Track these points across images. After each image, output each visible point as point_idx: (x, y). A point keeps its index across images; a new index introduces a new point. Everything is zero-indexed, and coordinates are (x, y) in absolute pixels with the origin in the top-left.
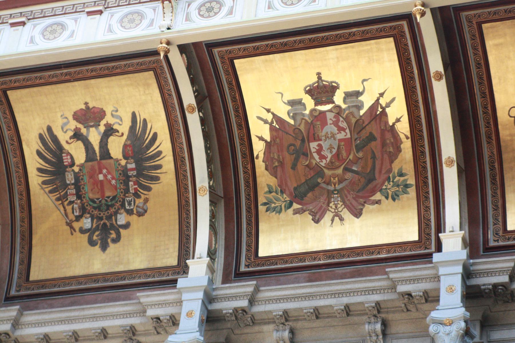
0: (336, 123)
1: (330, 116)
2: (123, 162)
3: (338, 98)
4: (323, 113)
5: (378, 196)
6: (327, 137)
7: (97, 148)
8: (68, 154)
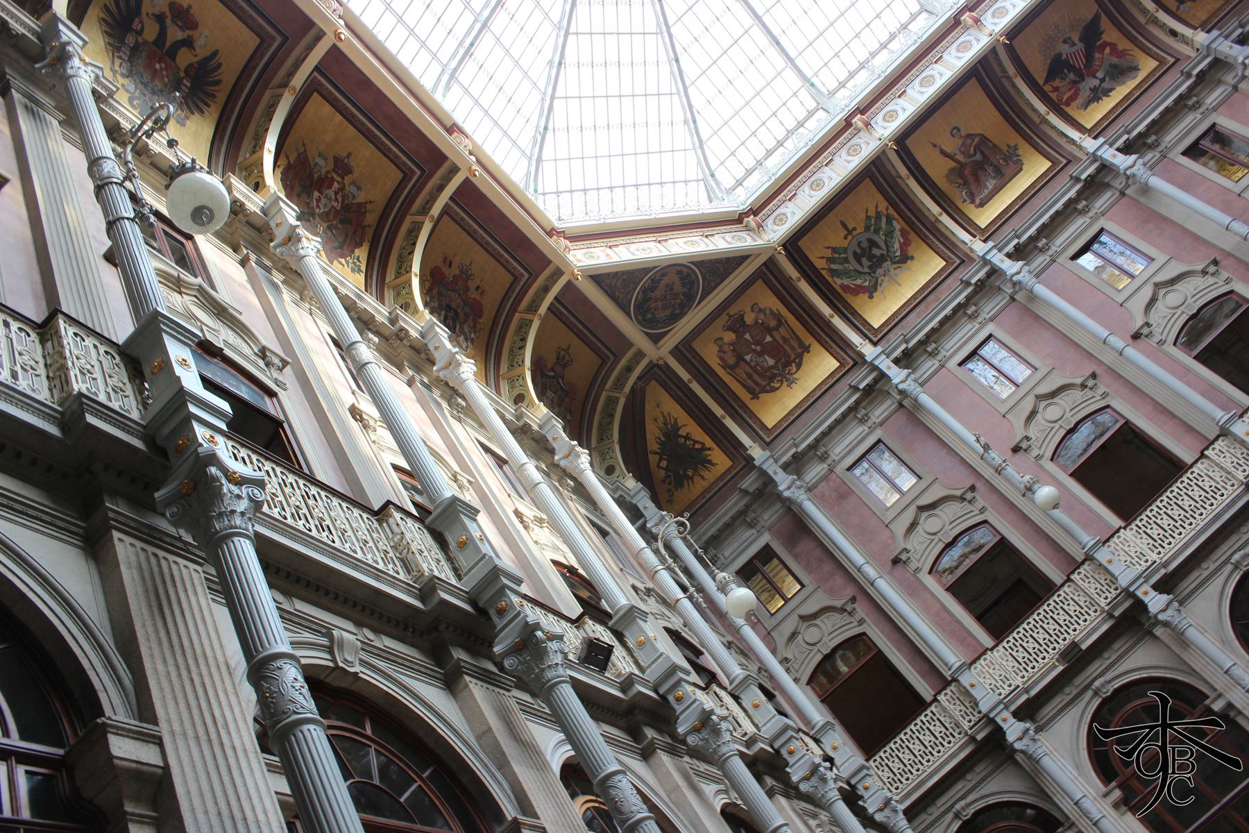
0: (336, 193)
1: (336, 185)
2: (182, 74)
3: (348, 179)
4: (333, 180)
5: (343, 261)
6: (326, 196)
7: (168, 44)
8: (142, 23)
